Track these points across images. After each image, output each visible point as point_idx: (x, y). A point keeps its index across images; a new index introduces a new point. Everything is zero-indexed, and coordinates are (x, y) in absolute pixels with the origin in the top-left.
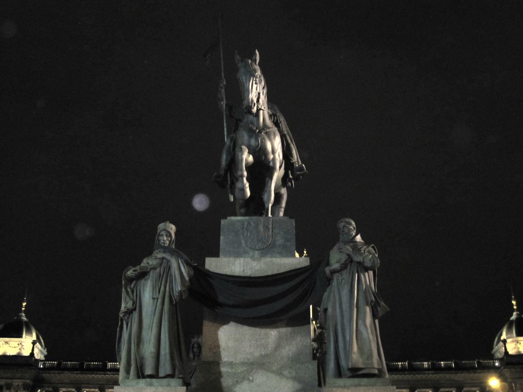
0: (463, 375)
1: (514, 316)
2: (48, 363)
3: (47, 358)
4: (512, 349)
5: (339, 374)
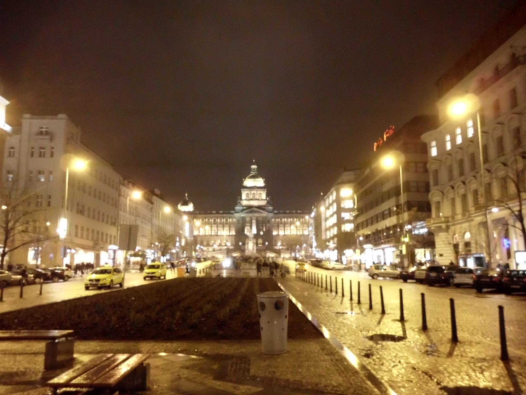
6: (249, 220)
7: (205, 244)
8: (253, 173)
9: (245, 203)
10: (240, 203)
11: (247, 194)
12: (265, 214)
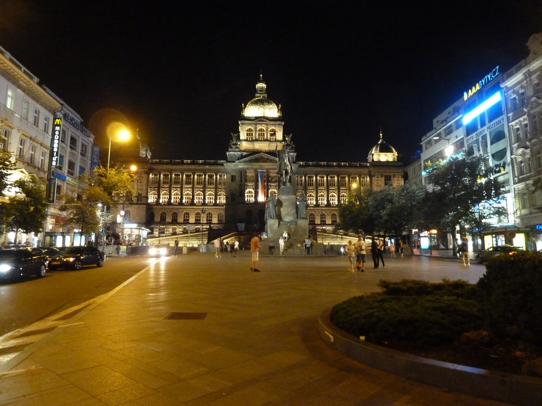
1: (379, 142)
2: (154, 161)
3: (153, 157)
4: (375, 159)
6: (252, 177)
7: (169, 219)
8: (259, 96)
9: (245, 145)
10: (236, 144)
11: (250, 130)
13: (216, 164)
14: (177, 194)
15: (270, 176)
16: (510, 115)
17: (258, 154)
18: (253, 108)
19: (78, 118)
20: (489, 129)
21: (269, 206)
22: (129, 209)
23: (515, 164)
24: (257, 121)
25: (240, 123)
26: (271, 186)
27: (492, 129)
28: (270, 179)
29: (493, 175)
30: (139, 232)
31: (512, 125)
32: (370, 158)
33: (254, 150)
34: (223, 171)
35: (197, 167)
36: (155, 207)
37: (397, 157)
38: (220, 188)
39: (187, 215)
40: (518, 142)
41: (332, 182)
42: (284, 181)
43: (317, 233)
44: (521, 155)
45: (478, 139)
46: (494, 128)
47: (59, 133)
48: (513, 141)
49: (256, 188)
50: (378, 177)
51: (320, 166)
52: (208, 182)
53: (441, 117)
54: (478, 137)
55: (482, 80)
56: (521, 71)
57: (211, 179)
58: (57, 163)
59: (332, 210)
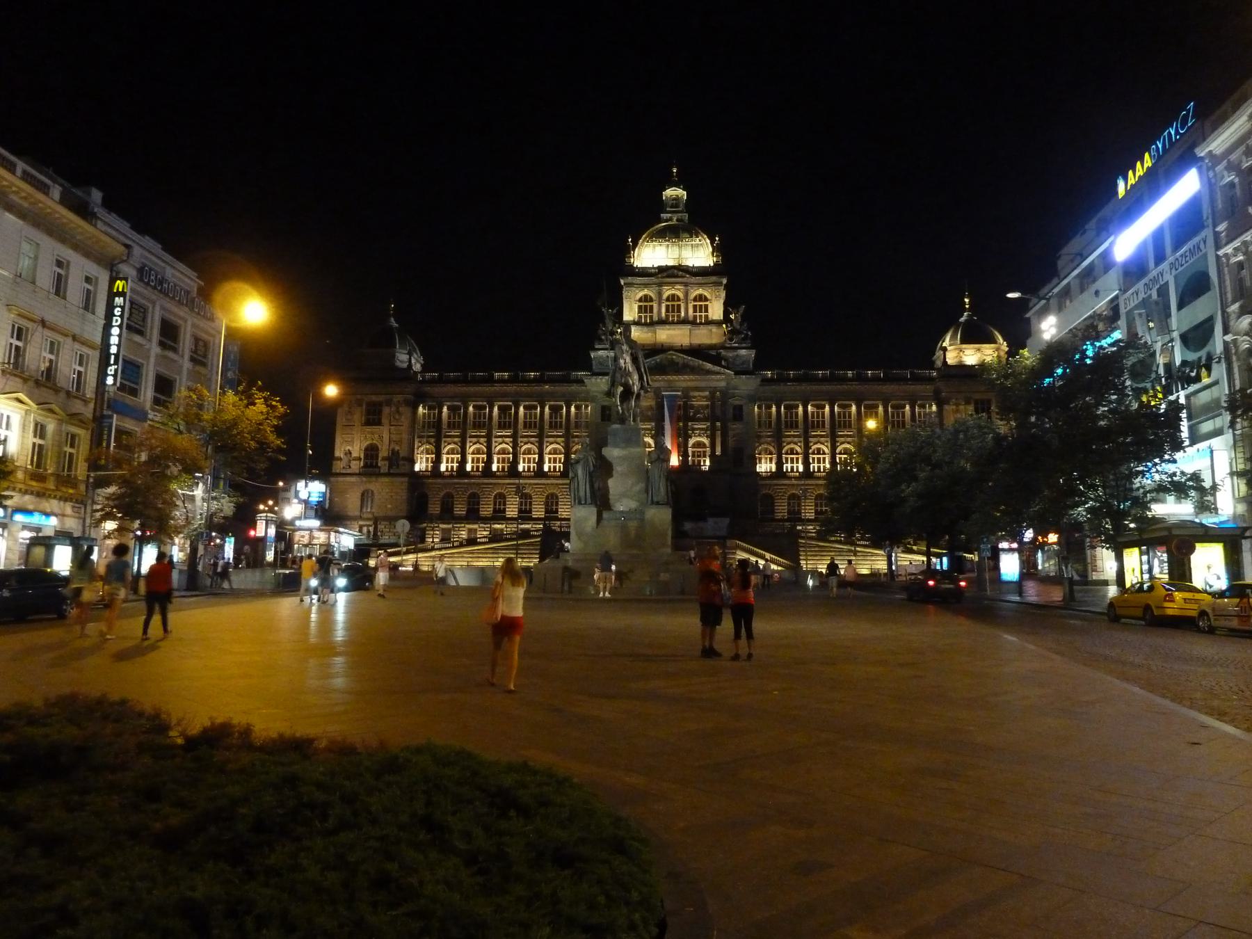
0: (892, 386)
1: (962, 320)
2: (428, 375)
3: (425, 368)
4: (951, 358)
5: (653, 503)
6: (650, 408)
7: (460, 510)
8: (669, 218)
11: (646, 298)
12: (721, 379)
13: (566, 380)
14: (478, 452)
15: (692, 407)
16: (1222, 227)
17: (661, 356)
18: (654, 246)
19: (192, 279)
20: (1173, 271)
21: (576, 475)
22: (372, 487)
23: (1234, 358)
24: (662, 278)
25: (622, 282)
26: (693, 430)
27: (1180, 269)
28: (691, 414)
29: (1183, 388)
30: (329, 538)
31: (1226, 255)
32: (939, 357)
33: (655, 344)
34: (583, 395)
35: (524, 388)
36: (430, 481)
37: (1007, 353)
38: (577, 436)
39: (502, 501)
40: (1241, 299)
41: (845, 417)
42: (618, 411)
43: (800, 541)
44: (1247, 334)
45: (1150, 296)
46: (1185, 265)
47: (123, 312)
48: (1229, 296)
49: (658, 434)
50: (957, 405)
51: (816, 380)
52: (551, 423)
53: (1075, 245)
54: (1149, 292)
55: (1158, 142)
56: (1242, 108)
57: (556, 413)
58: (115, 380)
59: (817, 485)
